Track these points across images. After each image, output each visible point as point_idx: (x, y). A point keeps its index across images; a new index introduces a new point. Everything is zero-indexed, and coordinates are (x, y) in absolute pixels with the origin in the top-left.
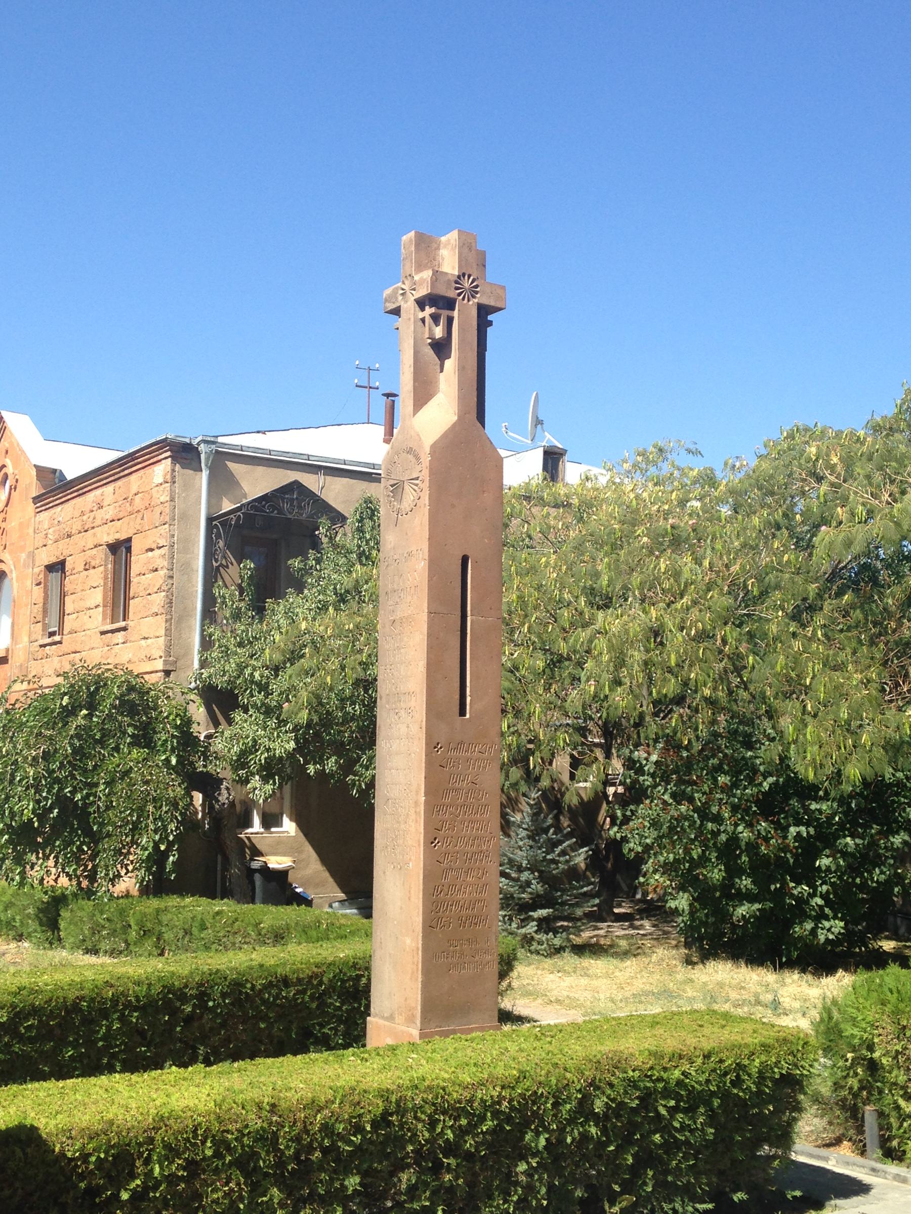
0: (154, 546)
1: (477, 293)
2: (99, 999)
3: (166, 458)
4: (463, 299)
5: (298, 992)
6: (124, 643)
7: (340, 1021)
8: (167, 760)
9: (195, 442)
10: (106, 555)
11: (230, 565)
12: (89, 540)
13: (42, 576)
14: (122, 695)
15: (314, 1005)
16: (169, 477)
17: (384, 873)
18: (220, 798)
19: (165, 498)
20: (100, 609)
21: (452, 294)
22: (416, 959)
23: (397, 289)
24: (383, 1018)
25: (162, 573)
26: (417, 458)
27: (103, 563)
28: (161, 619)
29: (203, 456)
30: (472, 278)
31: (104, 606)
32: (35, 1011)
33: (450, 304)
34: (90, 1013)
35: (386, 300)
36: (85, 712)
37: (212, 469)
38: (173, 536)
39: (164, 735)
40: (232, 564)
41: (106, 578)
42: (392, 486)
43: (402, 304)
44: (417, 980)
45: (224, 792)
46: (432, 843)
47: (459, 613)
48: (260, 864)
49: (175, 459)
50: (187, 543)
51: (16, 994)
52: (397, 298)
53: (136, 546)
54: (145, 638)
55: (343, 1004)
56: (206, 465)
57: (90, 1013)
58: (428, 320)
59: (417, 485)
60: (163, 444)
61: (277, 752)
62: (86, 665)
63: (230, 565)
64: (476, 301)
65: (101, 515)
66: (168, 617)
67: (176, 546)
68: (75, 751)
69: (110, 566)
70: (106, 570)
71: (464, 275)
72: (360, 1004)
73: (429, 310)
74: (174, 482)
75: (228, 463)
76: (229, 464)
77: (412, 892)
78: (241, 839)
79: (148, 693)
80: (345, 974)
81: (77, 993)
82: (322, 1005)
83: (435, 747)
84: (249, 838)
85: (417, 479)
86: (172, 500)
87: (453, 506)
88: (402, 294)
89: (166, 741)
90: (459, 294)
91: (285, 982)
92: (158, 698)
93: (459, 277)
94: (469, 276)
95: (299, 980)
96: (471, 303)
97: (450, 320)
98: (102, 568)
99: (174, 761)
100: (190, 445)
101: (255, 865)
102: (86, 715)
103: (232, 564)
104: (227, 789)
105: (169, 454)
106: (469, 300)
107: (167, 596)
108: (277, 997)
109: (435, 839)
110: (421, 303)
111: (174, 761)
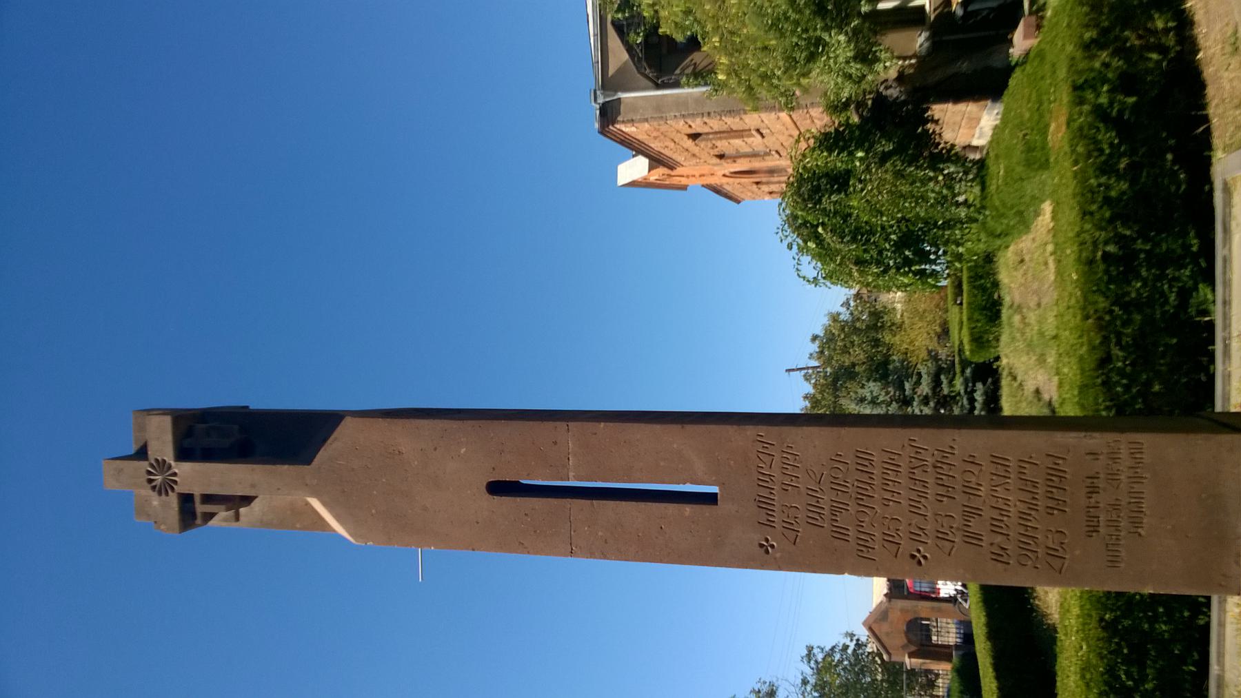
0: (687, 126)
1: (164, 461)
2: (1104, 600)
3: (616, 128)
4: (175, 482)
5: (1118, 343)
6: (769, 129)
8: (861, 159)
9: (598, 106)
10: (702, 140)
11: (693, 62)
12: (695, 150)
13: (729, 161)
14: (804, 200)
15: (1137, 317)
16: (629, 125)
18: (895, 96)
19: (646, 125)
20: (745, 139)
21: (173, 500)
25: (705, 119)
27: (709, 142)
28: (744, 117)
29: (608, 99)
30: (150, 469)
31: (743, 137)
32: (1111, 671)
33: (186, 500)
34: (1119, 608)
36: (820, 230)
37: (616, 91)
38: (675, 116)
39: (837, 162)
40: (692, 60)
41: (721, 139)
45: (889, 92)
46: (919, 563)
47: (567, 503)
48: (959, 7)
49: (614, 122)
50: (680, 103)
51: (1087, 685)
53: (690, 131)
54: (762, 121)
55: (1138, 277)
56: (614, 96)
57: (1119, 608)
60: (603, 131)
61: (848, 54)
62: (781, 227)
63: (693, 62)
64: (173, 463)
65: (672, 145)
66: (742, 112)
67: (683, 113)
68: (854, 240)
69: (711, 136)
70: (714, 139)
71: (150, 481)
72: (1141, 251)
74: (633, 120)
75: (609, 76)
76: (611, 71)
78: (936, 18)
79: (801, 174)
80: (1100, 279)
81: (1094, 623)
82: (1137, 305)
83: (767, 552)
84: (935, 10)
86: (646, 120)
87: (425, 509)
89: (842, 162)
90: (173, 489)
91: (1105, 362)
92: (804, 168)
93: (154, 488)
94: (149, 473)
95: (1106, 340)
96: (177, 471)
97: (208, 499)
98: (714, 142)
99: (860, 154)
100: (600, 109)
101: (960, 12)
102: (824, 229)
103: (692, 60)
104: (887, 88)
105: (611, 127)
106: (175, 474)
107: (725, 115)
108: (1121, 373)
109: (913, 557)
111: (860, 154)
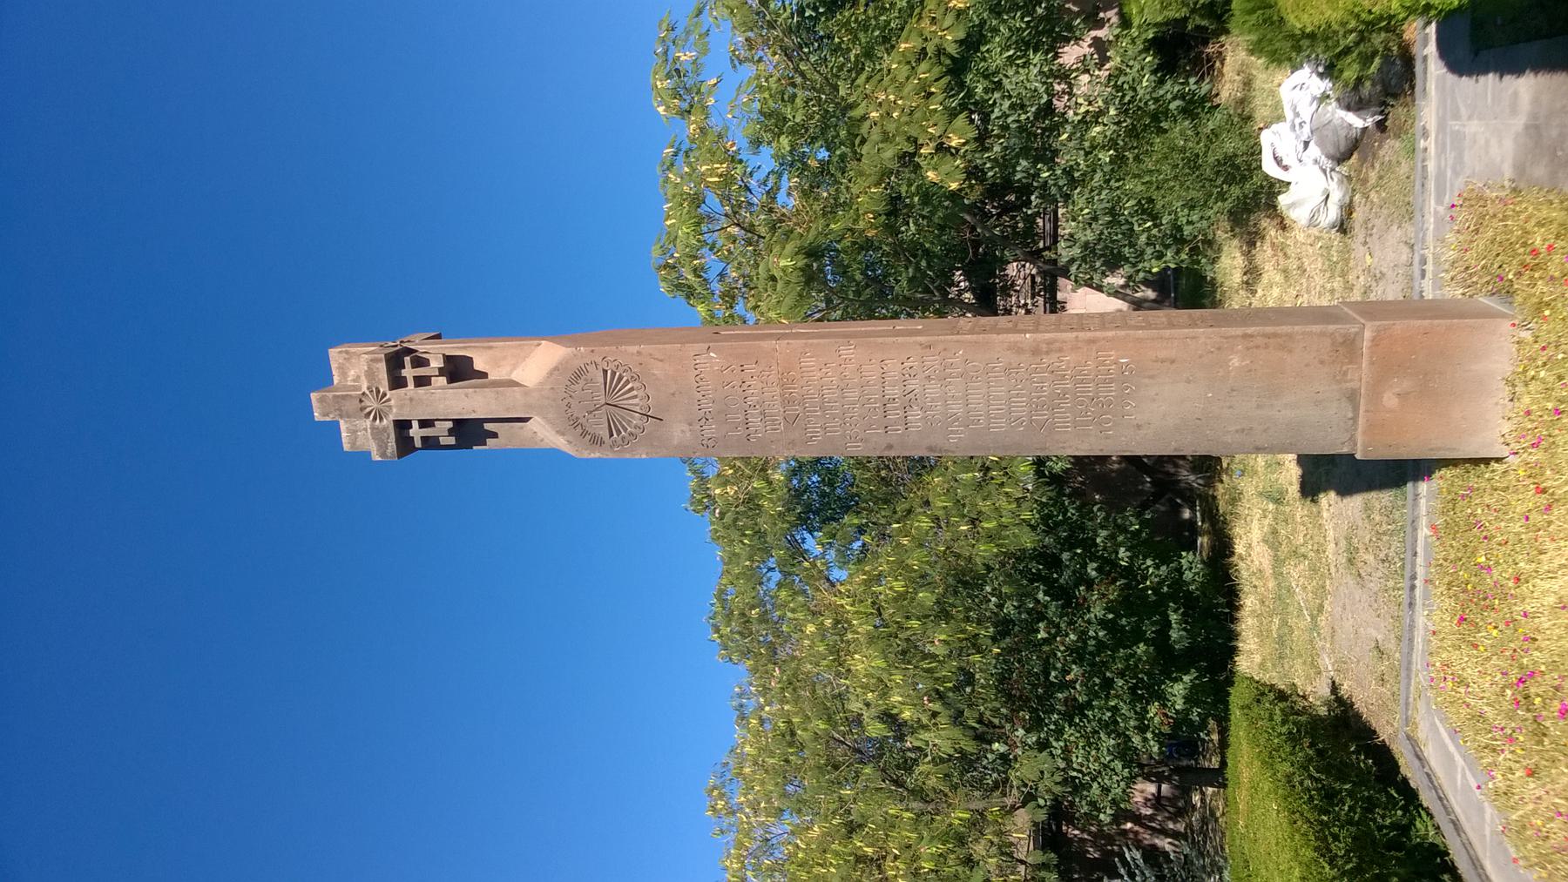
7: (1369, 810)
17: (1139, 427)
22: (1259, 341)
23: (373, 428)
24: (1355, 419)
26: (578, 374)
35: (383, 455)
42: (611, 435)
43: (392, 417)
44: (1290, 336)
52: (385, 429)
58: (421, 371)
59: (614, 373)
73: (408, 372)
77: (1163, 354)
85: (605, 372)
88: (381, 419)
110: (397, 382)
